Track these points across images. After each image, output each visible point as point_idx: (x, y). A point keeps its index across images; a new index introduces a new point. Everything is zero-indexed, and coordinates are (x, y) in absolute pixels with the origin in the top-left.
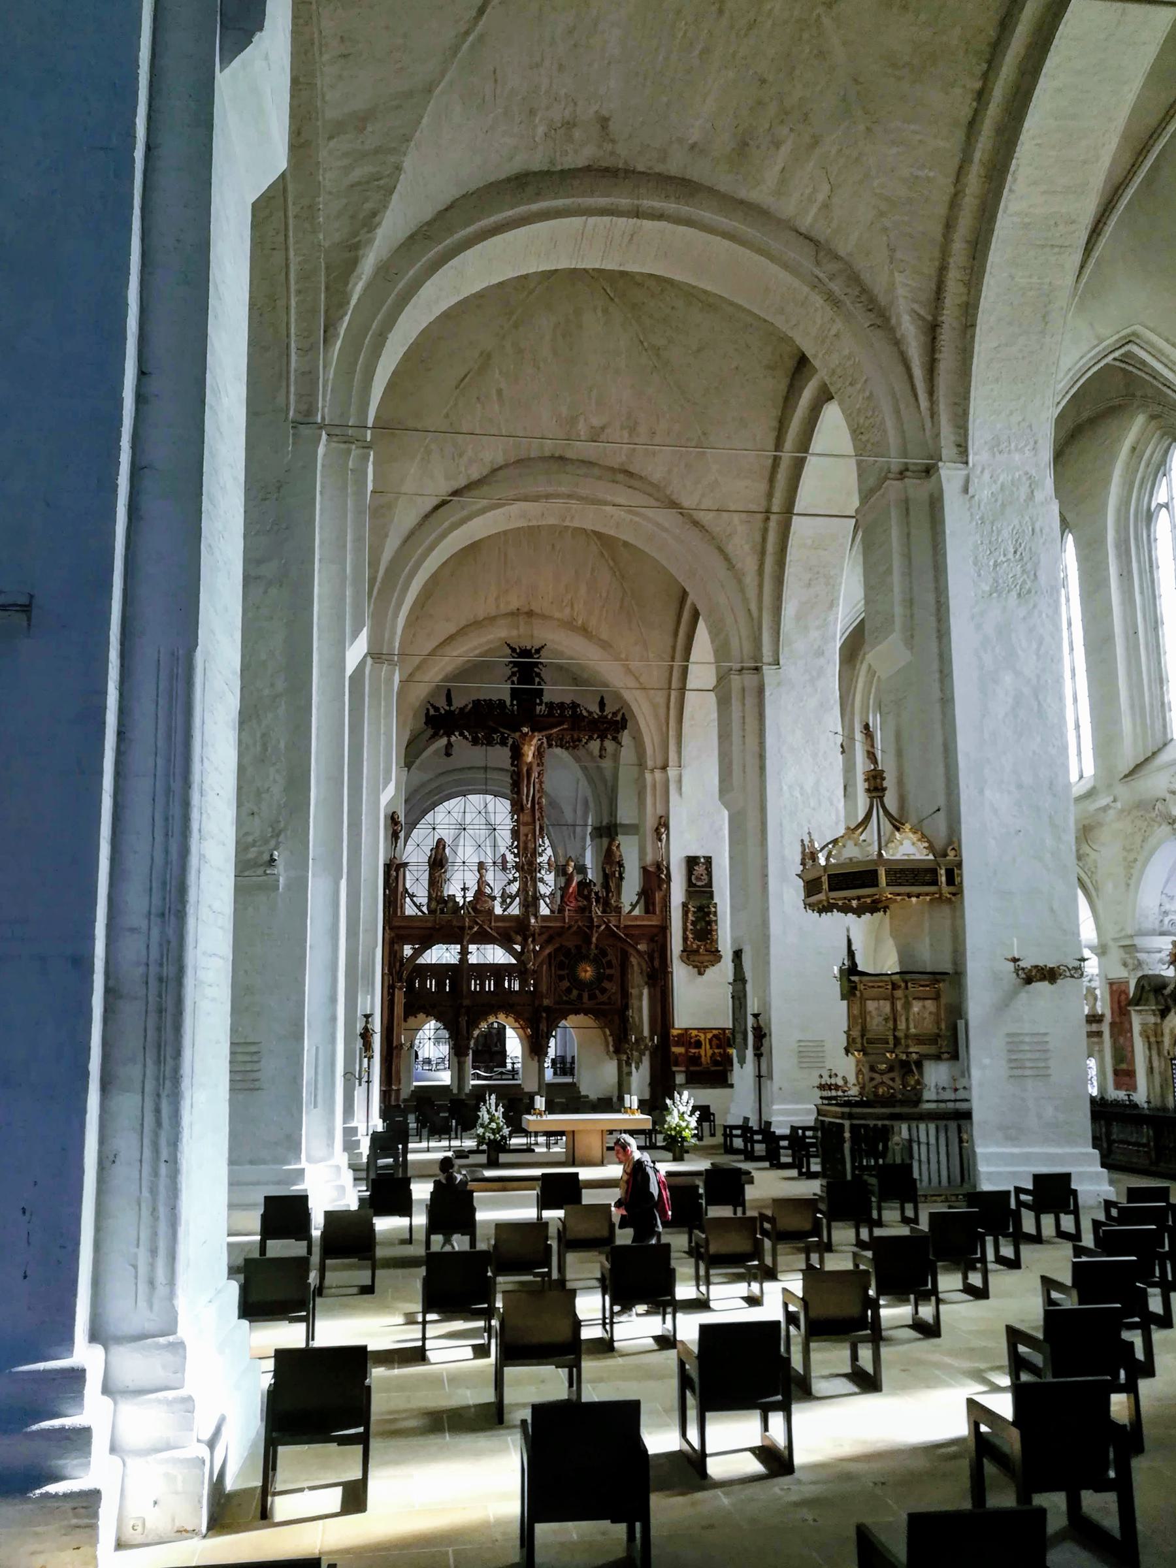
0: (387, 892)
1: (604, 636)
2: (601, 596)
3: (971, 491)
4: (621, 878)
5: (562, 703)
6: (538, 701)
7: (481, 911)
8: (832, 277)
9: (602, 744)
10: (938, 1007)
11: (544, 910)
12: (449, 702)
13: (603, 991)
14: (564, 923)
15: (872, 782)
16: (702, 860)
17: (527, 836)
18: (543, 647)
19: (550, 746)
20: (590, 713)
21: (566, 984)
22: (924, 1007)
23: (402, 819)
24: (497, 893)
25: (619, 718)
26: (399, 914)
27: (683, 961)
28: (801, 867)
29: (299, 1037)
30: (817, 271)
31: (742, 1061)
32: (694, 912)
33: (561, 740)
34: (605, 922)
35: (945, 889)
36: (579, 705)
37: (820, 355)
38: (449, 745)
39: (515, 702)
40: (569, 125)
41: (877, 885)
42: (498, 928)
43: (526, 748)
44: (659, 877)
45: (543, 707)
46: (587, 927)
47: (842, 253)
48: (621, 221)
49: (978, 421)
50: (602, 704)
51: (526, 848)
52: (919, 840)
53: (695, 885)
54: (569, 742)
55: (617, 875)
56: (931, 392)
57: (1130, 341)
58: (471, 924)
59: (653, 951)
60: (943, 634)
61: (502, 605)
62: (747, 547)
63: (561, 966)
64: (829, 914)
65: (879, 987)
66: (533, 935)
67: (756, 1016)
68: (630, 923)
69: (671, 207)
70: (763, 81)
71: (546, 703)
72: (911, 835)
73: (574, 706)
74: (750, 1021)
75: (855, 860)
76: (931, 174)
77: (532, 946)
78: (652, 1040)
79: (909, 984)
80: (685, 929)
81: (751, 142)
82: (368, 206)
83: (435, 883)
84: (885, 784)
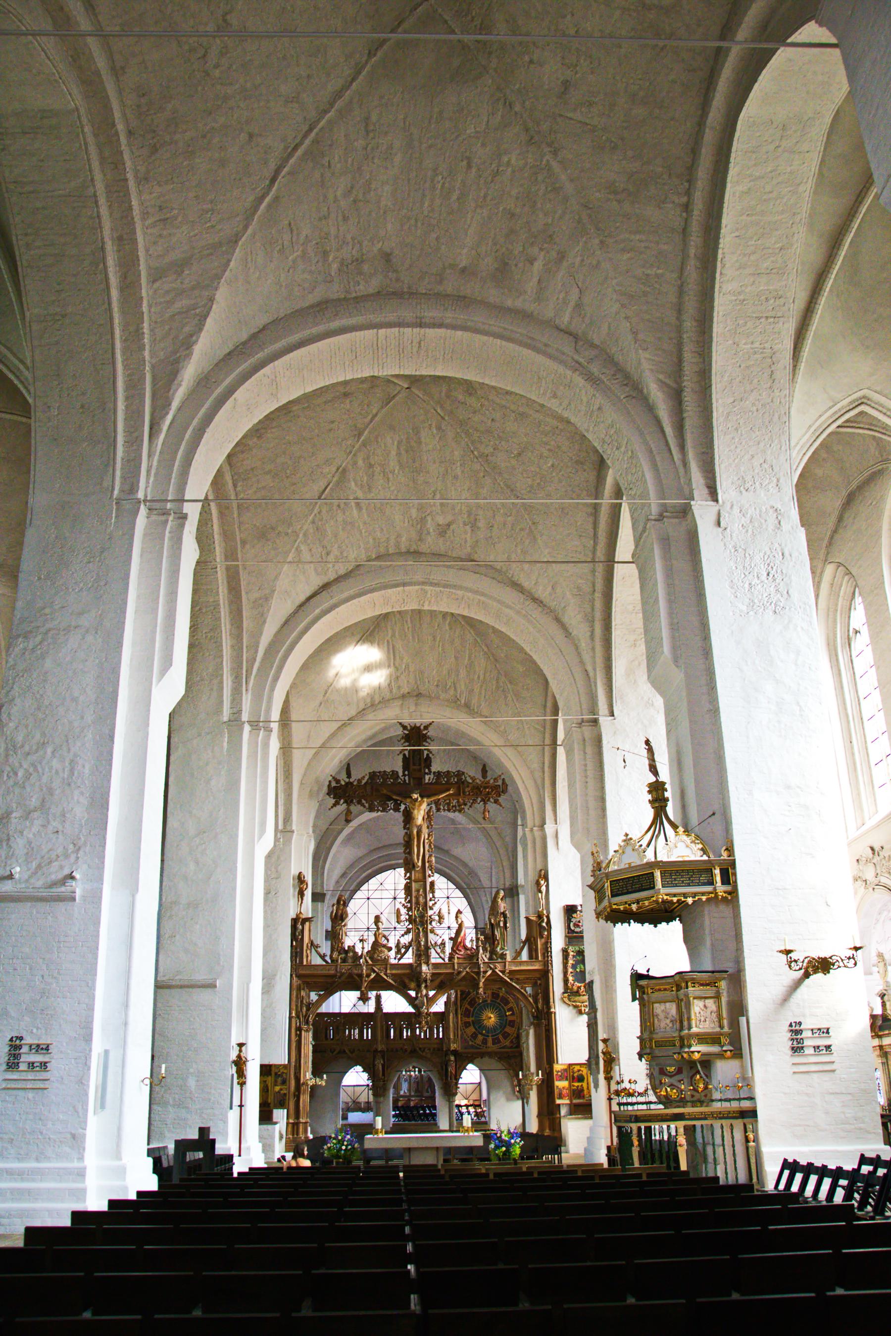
2: (479, 677)
3: (722, 524)
5: (448, 772)
6: (427, 771)
8: (590, 361)
10: (719, 1008)
11: (435, 958)
12: (349, 775)
13: (506, 1035)
15: (654, 793)
17: (418, 891)
19: (438, 810)
20: (473, 779)
21: (471, 1030)
22: (705, 1006)
23: (309, 879)
24: (392, 944)
25: (500, 783)
26: (305, 963)
27: (564, 1002)
28: (592, 879)
29: (88, 1038)
30: (576, 357)
31: (596, 1086)
32: (574, 956)
33: (448, 804)
34: (491, 968)
35: (721, 888)
36: (463, 773)
37: (591, 429)
39: (406, 773)
40: (359, 261)
41: (654, 888)
42: (393, 975)
43: (416, 812)
44: (540, 925)
45: (432, 776)
46: (474, 972)
47: (596, 342)
48: (408, 331)
49: (723, 466)
50: (484, 771)
51: (417, 903)
52: (693, 842)
53: (573, 932)
54: (455, 806)
55: (502, 924)
56: (682, 447)
57: (862, 403)
58: (369, 972)
60: (707, 652)
62: (579, 617)
63: (467, 1013)
64: (626, 925)
65: (665, 990)
66: (426, 981)
67: (605, 1041)
68: (514, 968)
69: (449, 316)
70: (513, 215)
71: (434, 773)
72: (685, 837)
73: (459, 774)
74: (601, 1046)
75: (633, 865)
76: (660, 271)
77: (424, 992)
78: (538, 1075)
79: (689, 984)
81: (510, 262)
82: (187, 329)
83: (334, 936)
84: (667, 794)
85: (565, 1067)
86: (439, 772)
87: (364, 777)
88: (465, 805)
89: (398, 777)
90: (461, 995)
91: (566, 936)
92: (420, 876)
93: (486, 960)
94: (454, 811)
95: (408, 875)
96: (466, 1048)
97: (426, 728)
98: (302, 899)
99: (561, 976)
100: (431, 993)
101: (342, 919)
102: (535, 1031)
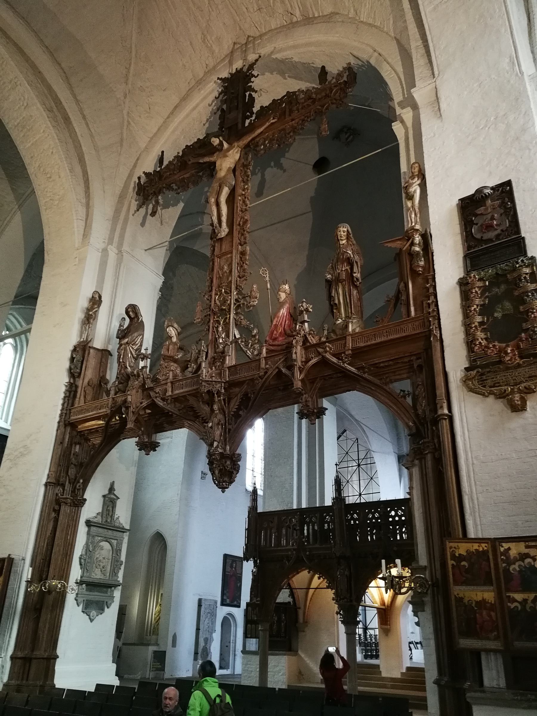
27: (471, 390)
34: (319, 354)
53: (481, 241)
61: (216, 49)
85: (484, 546)
99: (461, 336)
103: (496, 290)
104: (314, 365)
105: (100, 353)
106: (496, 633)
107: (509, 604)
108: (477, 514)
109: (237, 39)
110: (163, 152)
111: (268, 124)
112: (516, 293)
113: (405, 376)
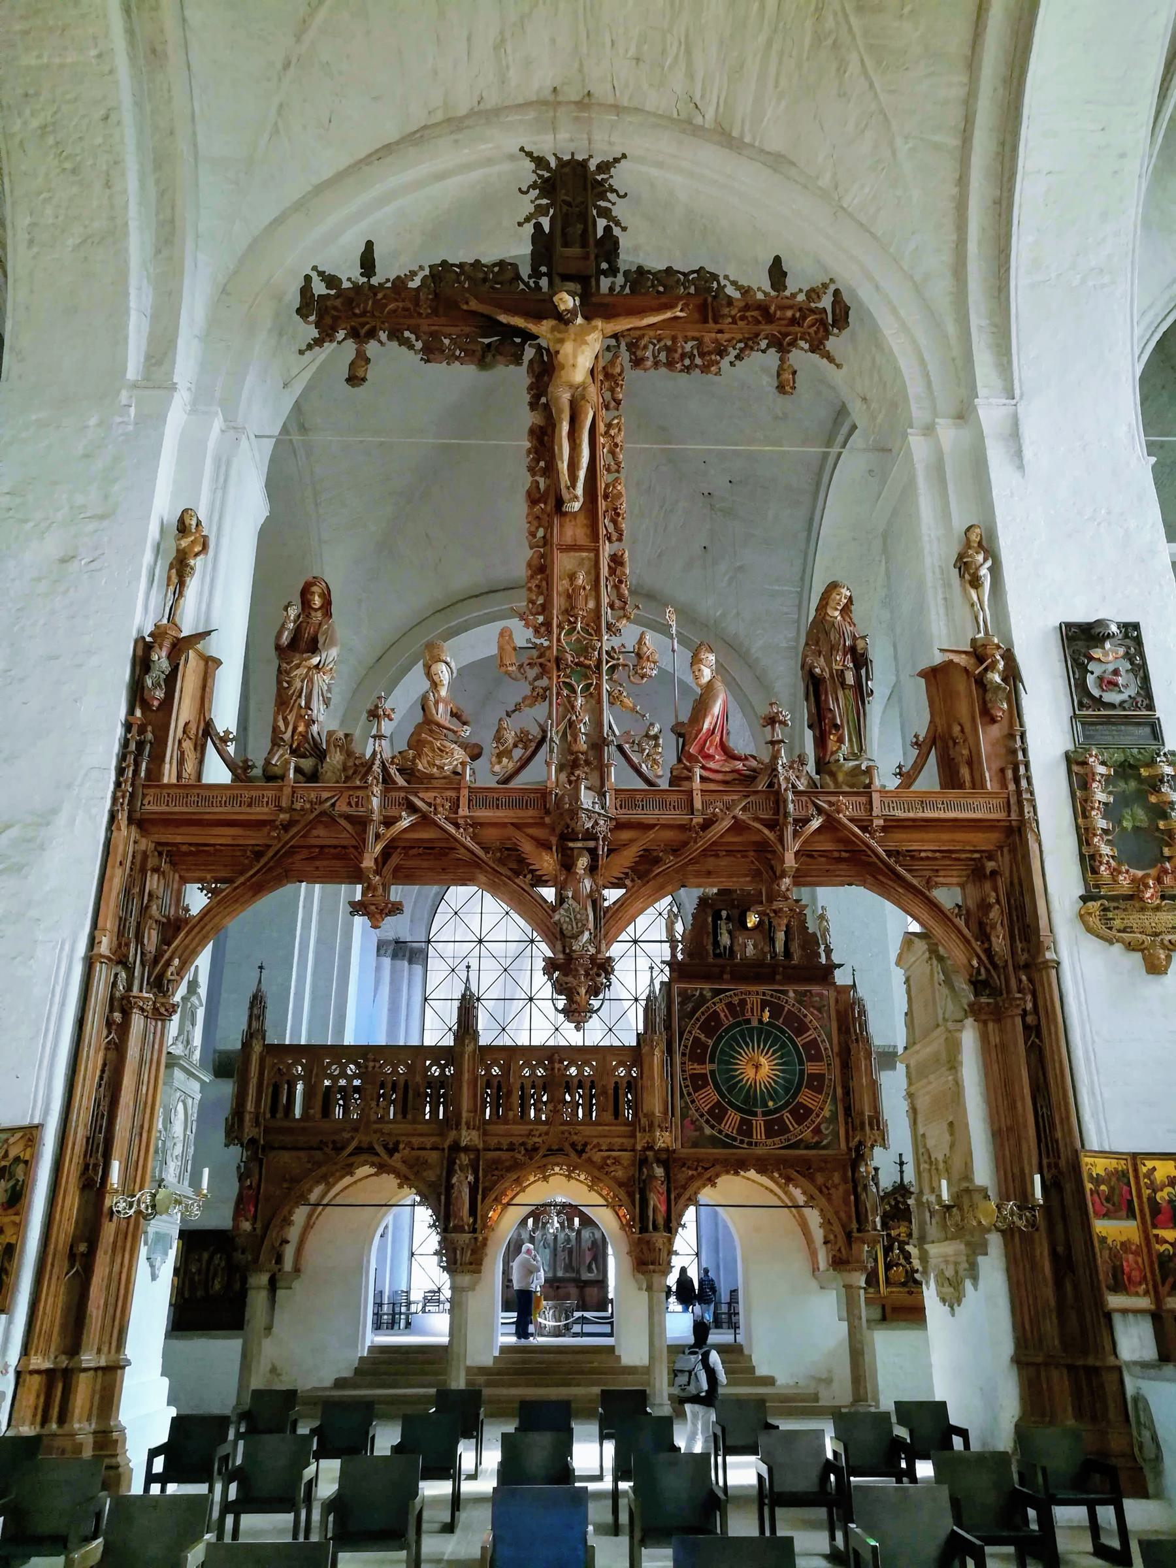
0: (138, 713)
1: (775, 141)
4: (861, 693)
5: (669, 271)
6: (604, 266)
7: (431, 777)
9: (782, 359)
12: (368, 262)
13: (802, 1114)
14: (692, 811)
16: (1114, 628)
17: (572, 577)
18: (617, 160)
19: (637, 362)
20: (746, 291)
21: (709, 1096)
25: (826, 302)
27: (1089, 930)
32: (1108, 779)
34: (820, 810)
36: (715, 277)
38: (362, 359)
42: (476, 824)
45: (620, 280)
50: (777, 272)
51: (570, 611)
53: (1099, 702)
55: (850, 678)
58: (393, 812)
59: (985, 907)
63: (697, 1053)
68: (899, 814)
71: (626, 273)
80: (1084, 835)
85: (1121, 1165)
86: (641, 271)
87: (413, 274)
88: (722, 353)
89: (518, 277)
90: (681, 1004)
91: (1075, 716)
92: (574, 531)
93: (801, 788)
94: (687, 369)
95: (541, 533)
96: (695, 1145)
97: (604, 167)
98: (182, 583)
100: (612, 895)
101: (313, 648)
102: (984, 1038)
103: (1122, 785)
104: (818, 830)
105: (202, 663)
106: (1144, 1286)
107: (1158, 1246)
108: (1101, 1116)
109: (564, 84)
110: (369, 245)
111: (668, 315)
112: (1153, 799)
113: (955, 880)
